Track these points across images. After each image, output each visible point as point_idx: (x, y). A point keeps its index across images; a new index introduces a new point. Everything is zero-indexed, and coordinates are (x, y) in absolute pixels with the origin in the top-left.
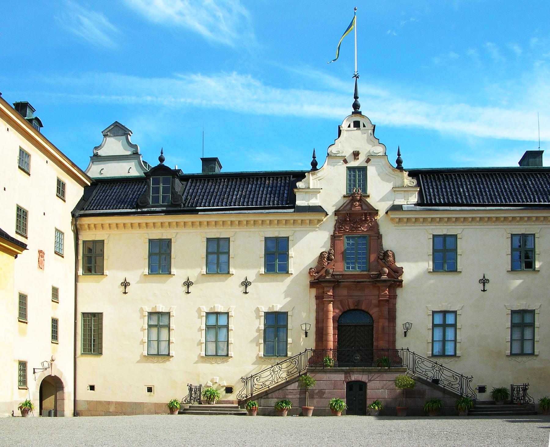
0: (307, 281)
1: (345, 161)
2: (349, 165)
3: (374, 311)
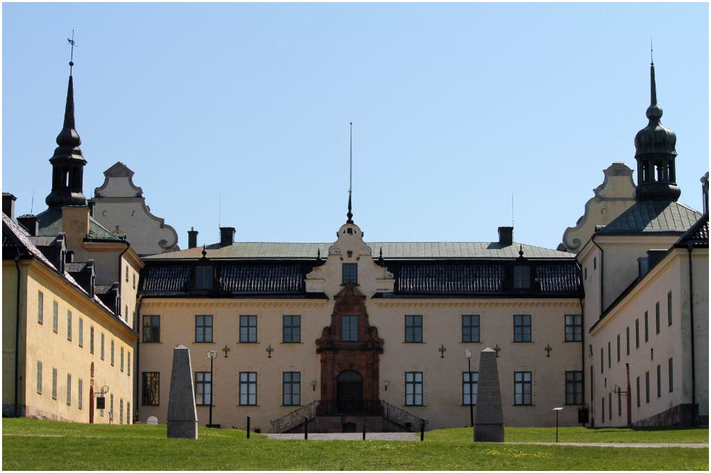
0: (314, 347)
1: (342, 259)
2: (344, 262)
3: (363, 372)
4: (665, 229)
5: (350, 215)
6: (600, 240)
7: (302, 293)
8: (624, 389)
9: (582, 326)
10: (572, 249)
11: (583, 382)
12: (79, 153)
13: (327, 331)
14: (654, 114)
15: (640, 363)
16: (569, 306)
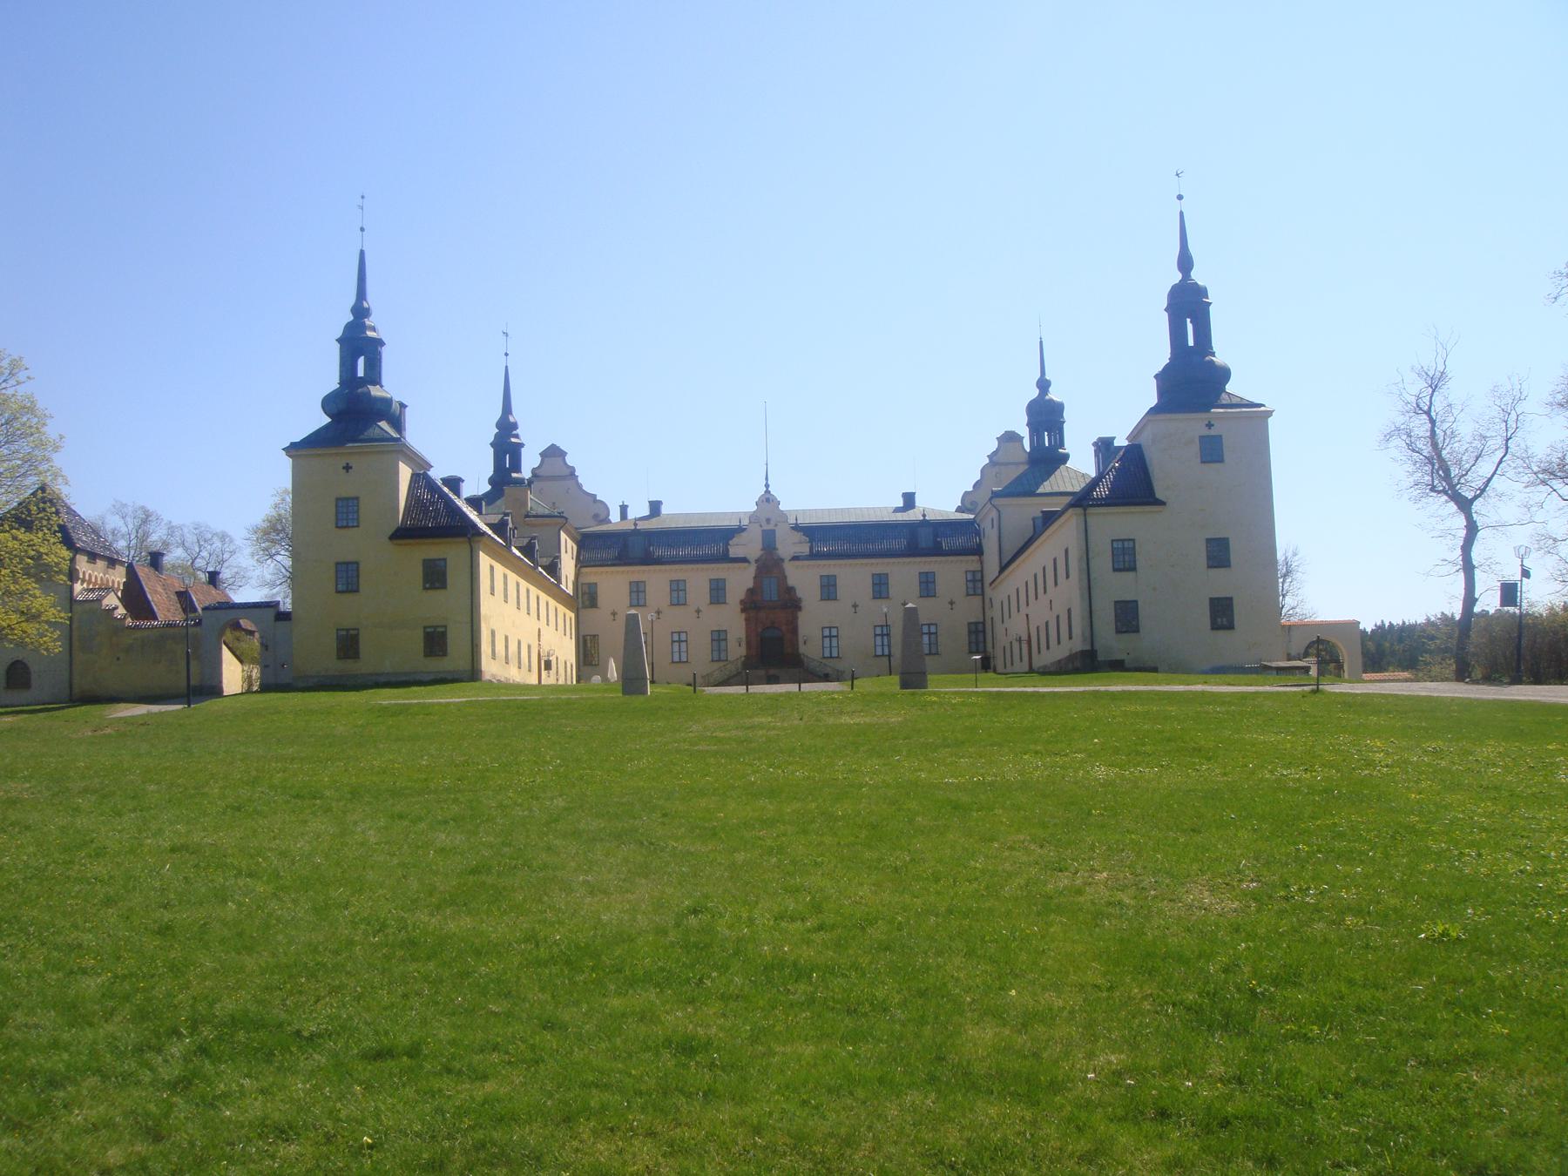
0: (738, 608)
4: (1056, 489)
5: (767, 486)
6: (996, 501)
7: (725, 558)
8: (1025, 637)
9: (982, 580)
10: (969, 511)
11: (984, 631)
12: (517, 436)
13: (750, 591)
14: (1043, 385)
15: (1039, 613)
16: (971, 562)
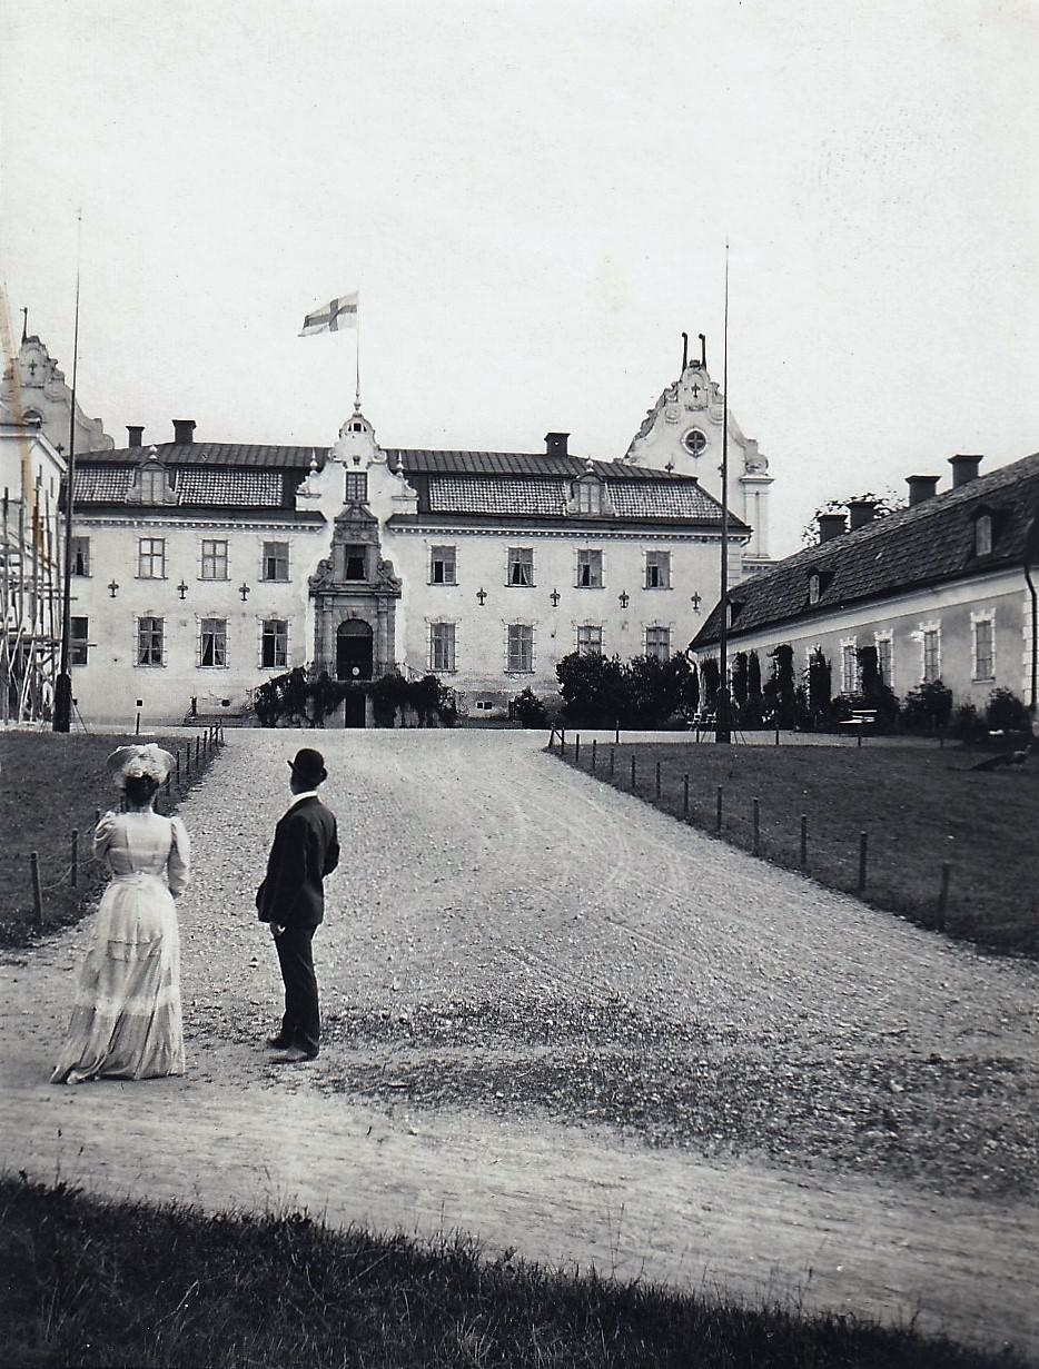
0: (305, 590)
1: (345, 464)
2: (349, 470)
3: (373, 622)
5: (357, 406)
